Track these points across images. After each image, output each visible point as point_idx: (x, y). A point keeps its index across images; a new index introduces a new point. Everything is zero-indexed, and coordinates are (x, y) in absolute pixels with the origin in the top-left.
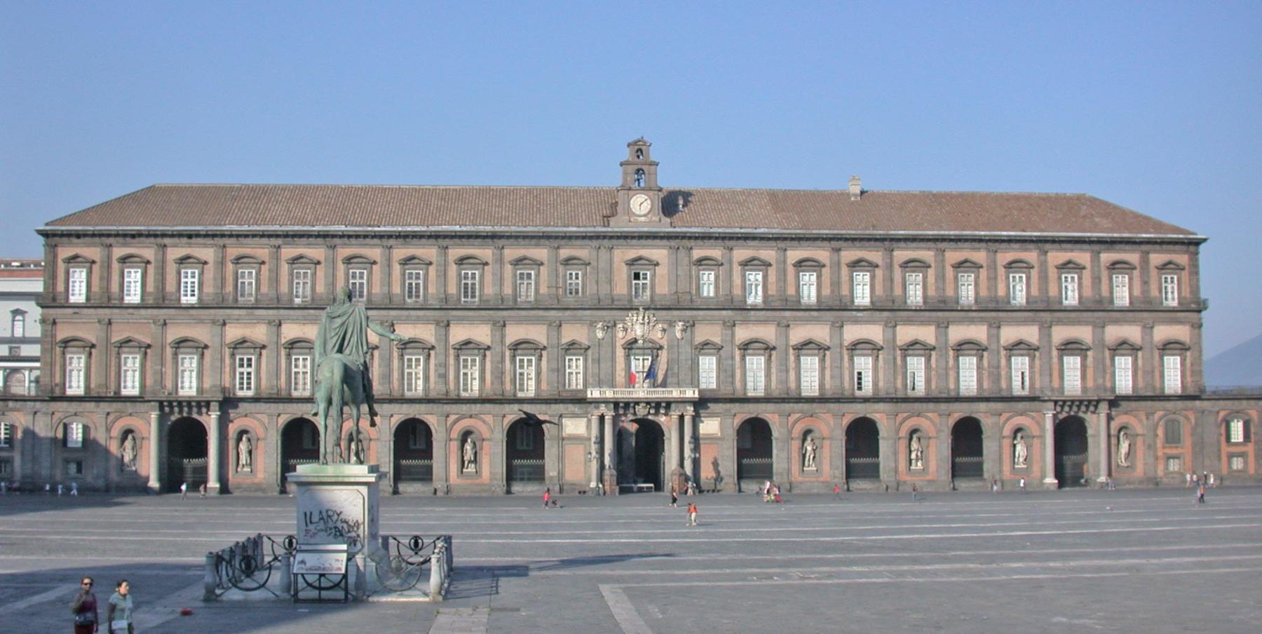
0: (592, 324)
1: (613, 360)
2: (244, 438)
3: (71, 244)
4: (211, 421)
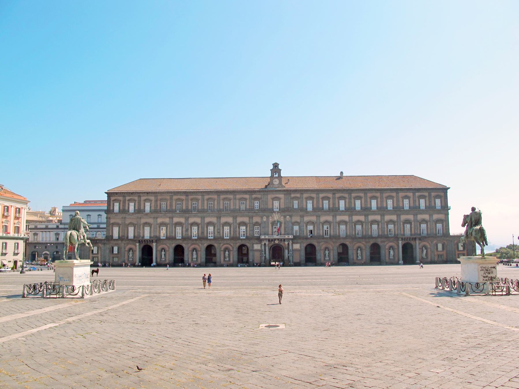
0: (262, 217)
1: (268, 227)
3: (114, 196)
4: (154, 245)
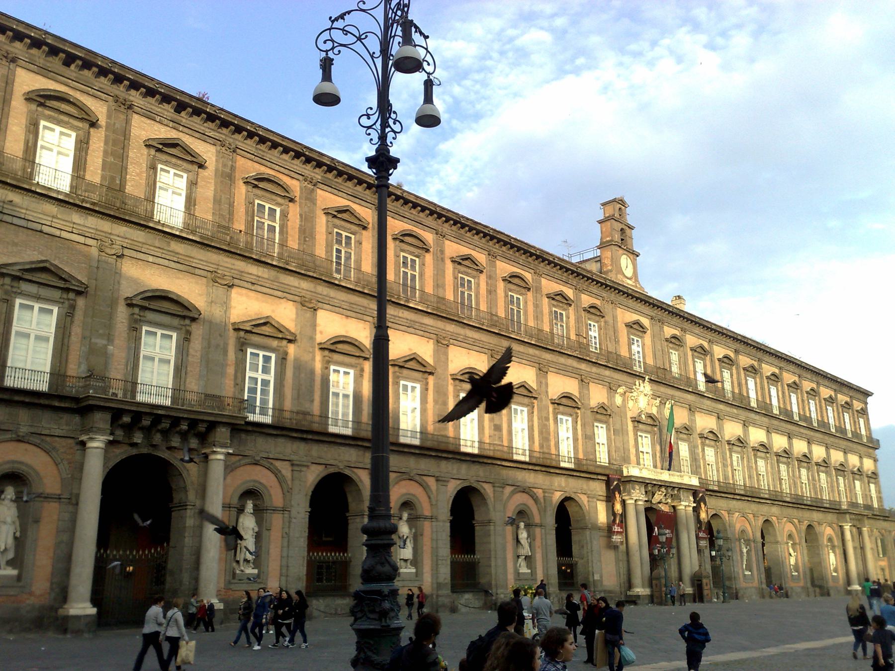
2: (250, 506)
